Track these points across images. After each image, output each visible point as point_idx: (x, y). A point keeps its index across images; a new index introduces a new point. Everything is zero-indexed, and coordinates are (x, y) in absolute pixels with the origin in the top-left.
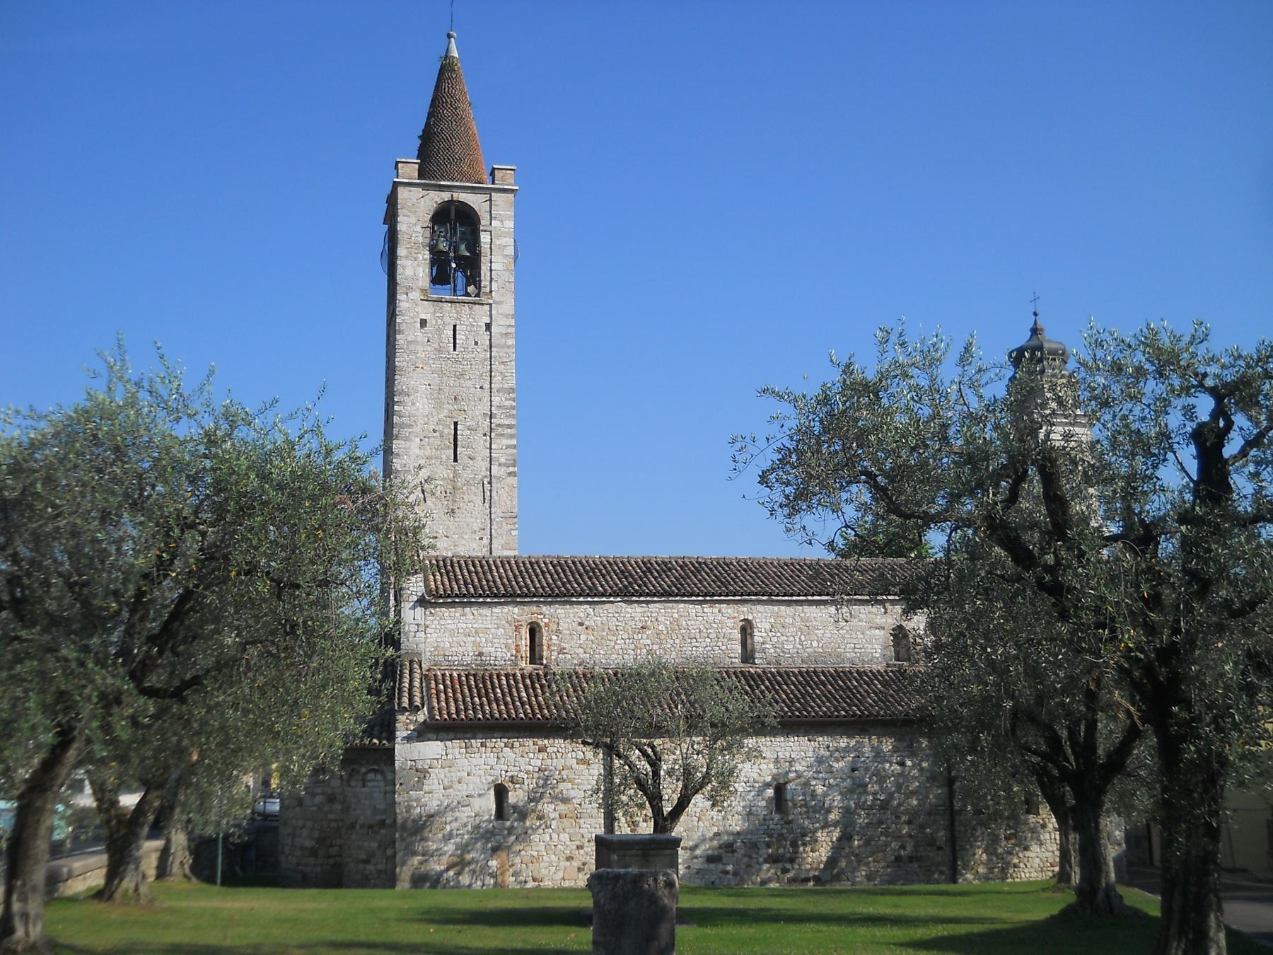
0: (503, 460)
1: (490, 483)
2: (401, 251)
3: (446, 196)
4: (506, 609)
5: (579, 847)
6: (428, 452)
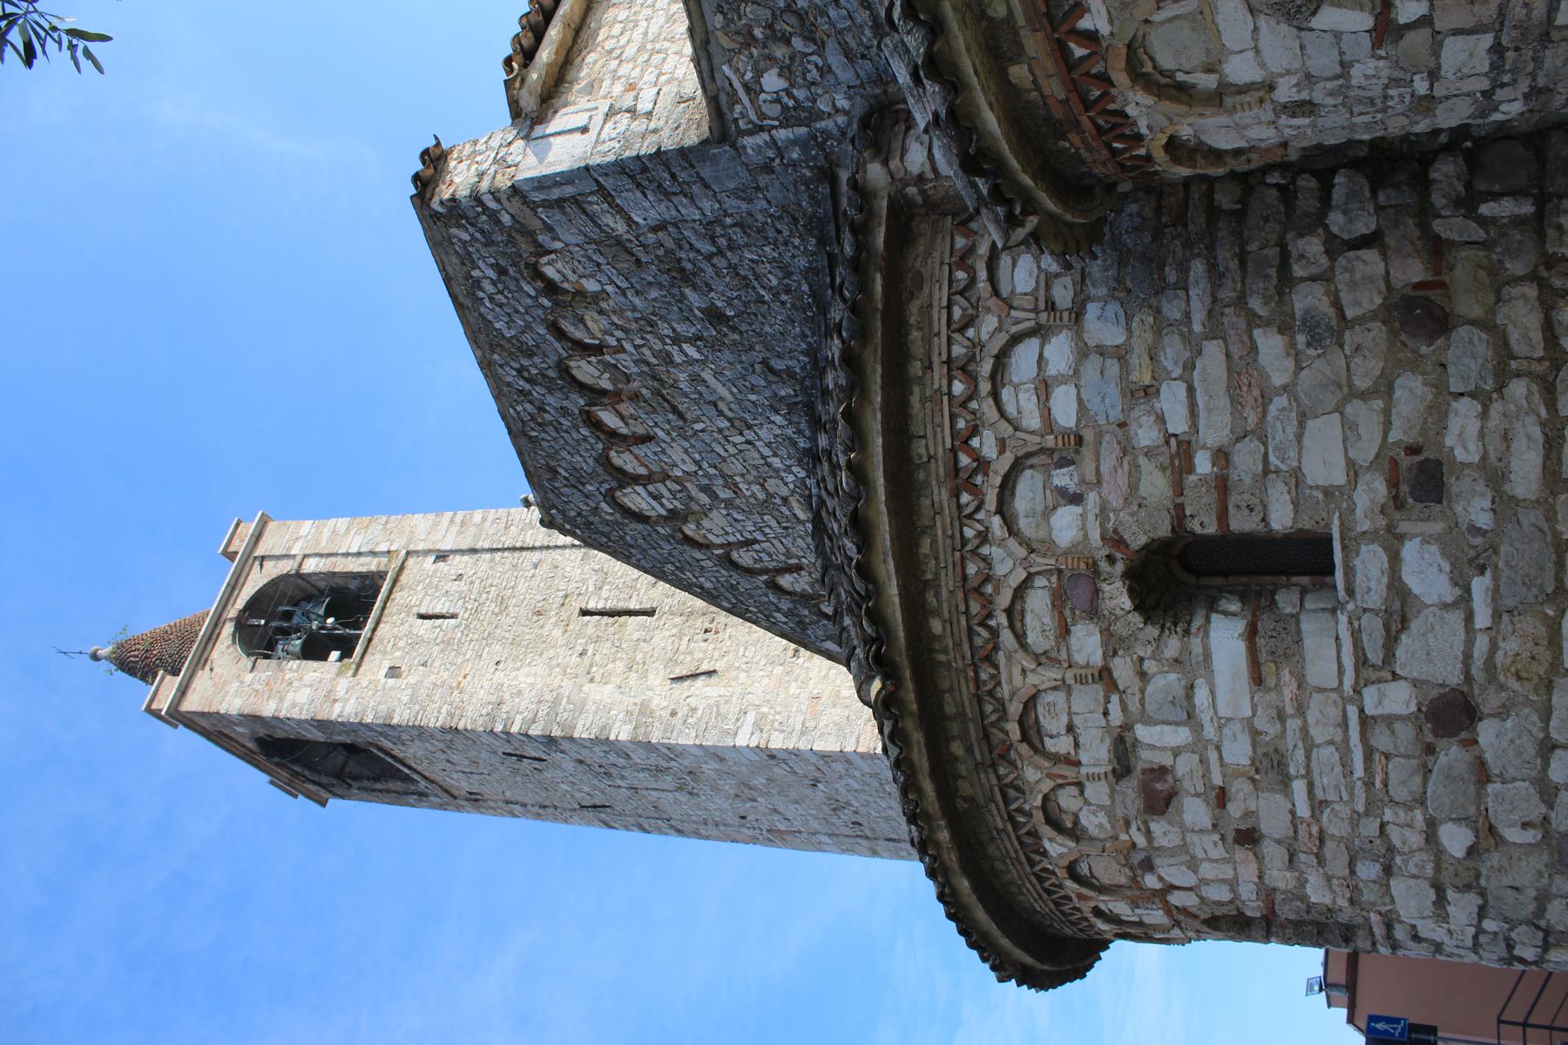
6: (620, 666)
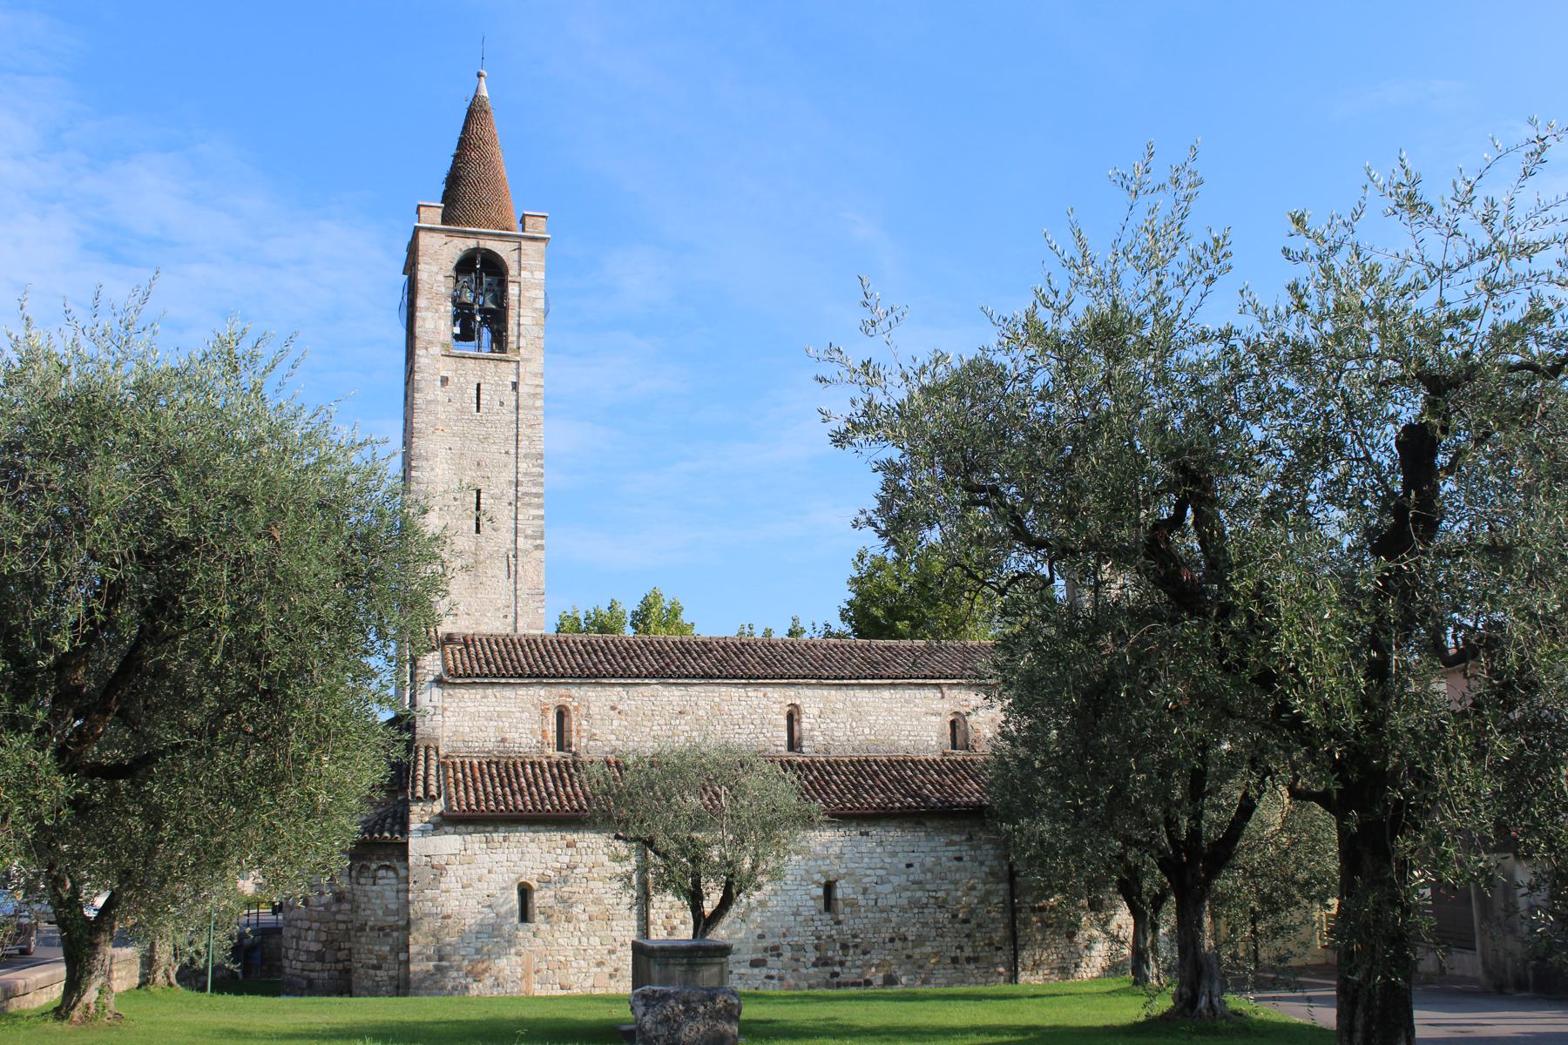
0: (529, 532)
1: (515, 556)
2: (421, 302)
3: (472, 243)
4: (532, 691)
5: (611, 952)
